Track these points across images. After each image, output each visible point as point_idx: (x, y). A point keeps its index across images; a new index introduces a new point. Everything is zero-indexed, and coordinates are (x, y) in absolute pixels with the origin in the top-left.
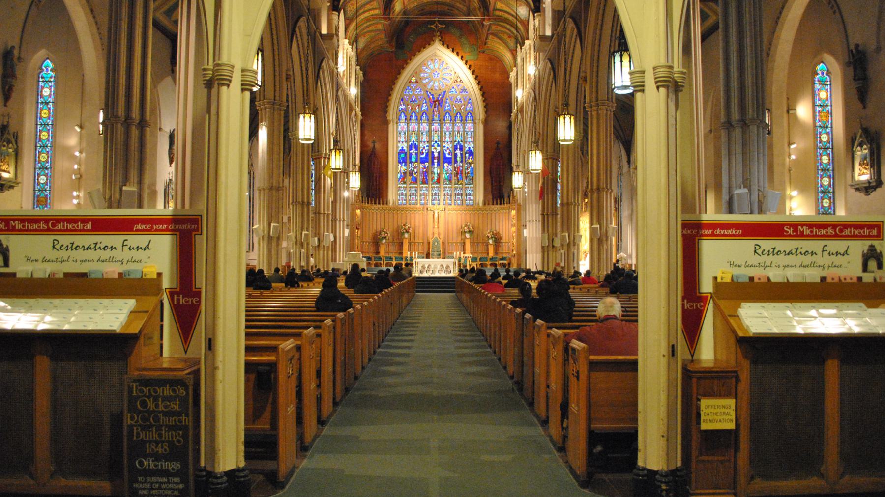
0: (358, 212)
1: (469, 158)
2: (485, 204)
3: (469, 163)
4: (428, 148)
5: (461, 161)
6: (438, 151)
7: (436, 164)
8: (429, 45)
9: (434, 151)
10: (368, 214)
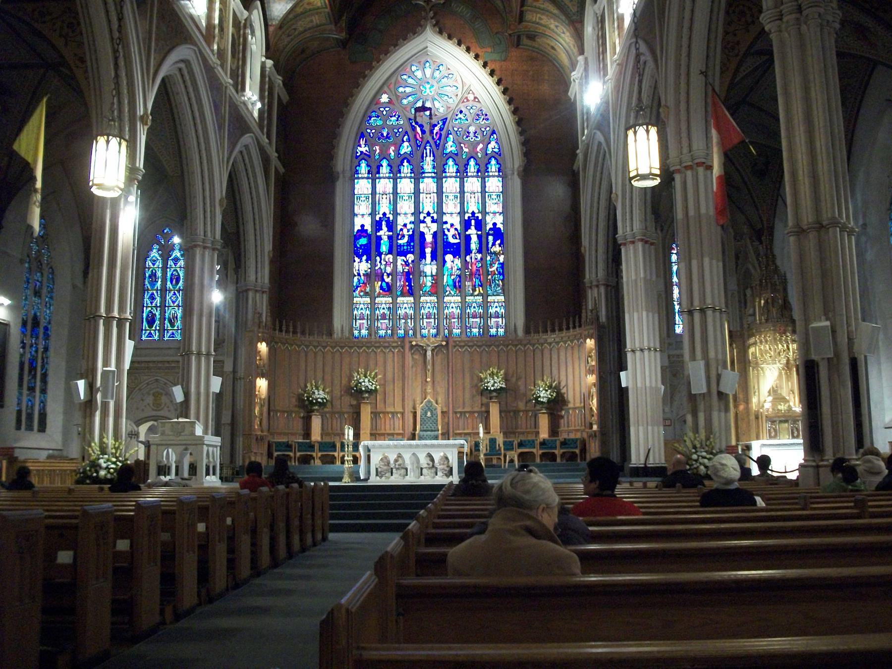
0: (263, 347)
1: (494, 244)
3: (495, 253)
4: (412, 226)
5: (480, 251)
6: (432, 232)
7: (428, 256)
8: (414, 34)
9: (425, 230)
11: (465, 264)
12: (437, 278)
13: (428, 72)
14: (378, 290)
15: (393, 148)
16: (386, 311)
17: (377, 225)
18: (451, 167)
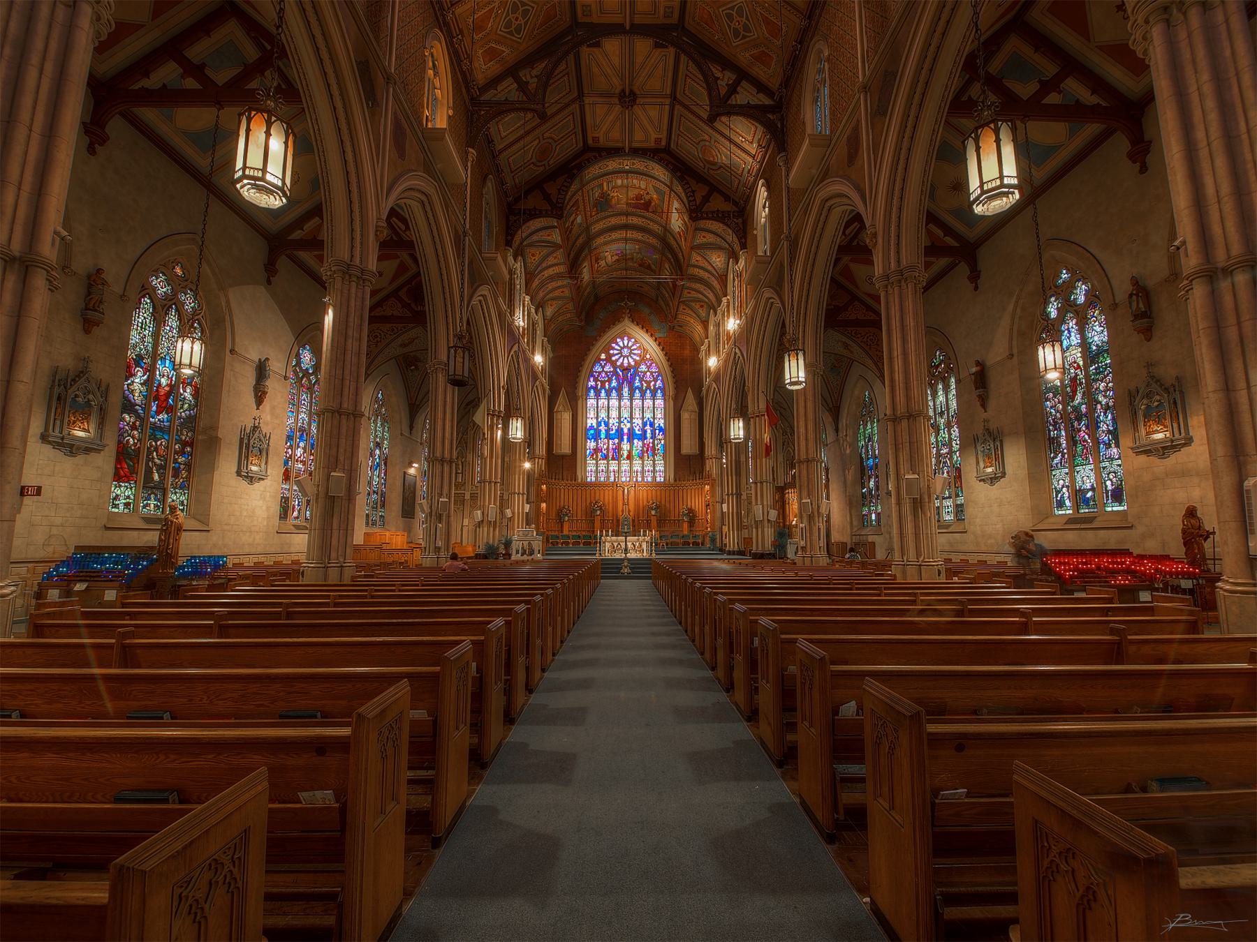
2: (675, 480)
7: (625, 440)
9: (624, 427)
10: (555, 490)
11: (644, 444)
12: (630, 452)
13: (626, 342)
14: (599, 457)
15: (607, 383)
16: (604, 469)
17: (599, 424)
18: (637, 394)
